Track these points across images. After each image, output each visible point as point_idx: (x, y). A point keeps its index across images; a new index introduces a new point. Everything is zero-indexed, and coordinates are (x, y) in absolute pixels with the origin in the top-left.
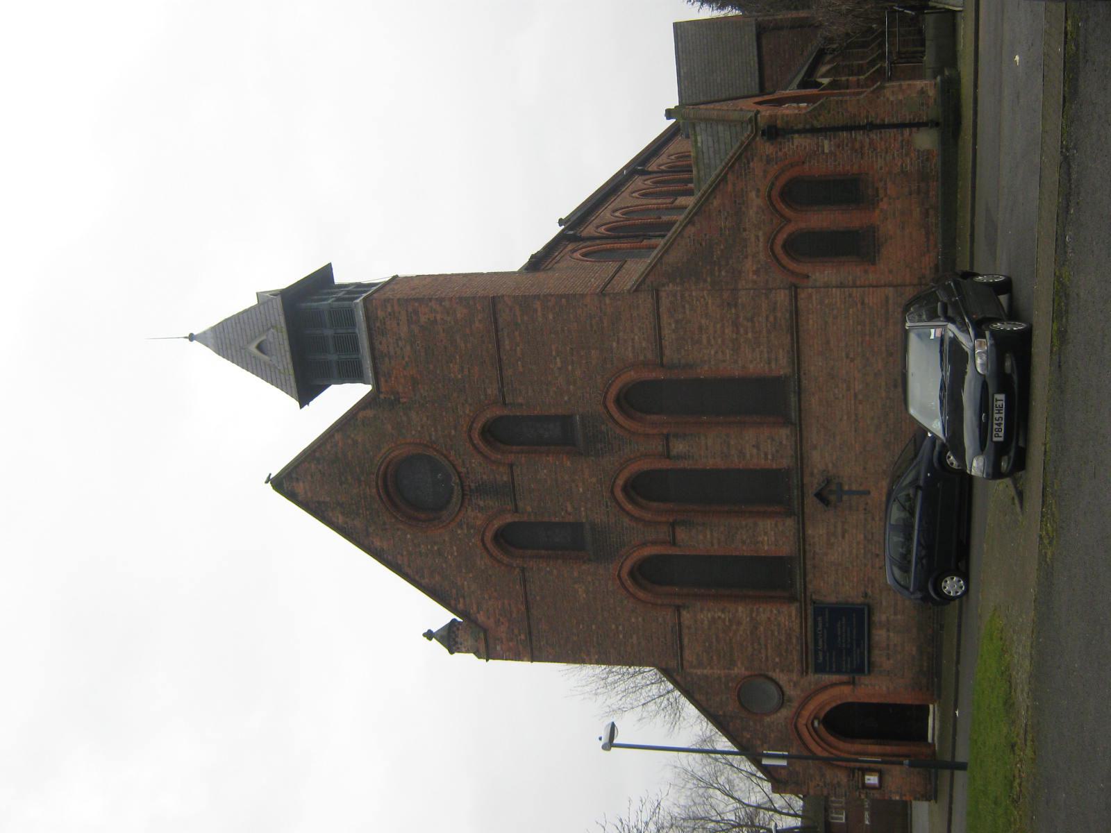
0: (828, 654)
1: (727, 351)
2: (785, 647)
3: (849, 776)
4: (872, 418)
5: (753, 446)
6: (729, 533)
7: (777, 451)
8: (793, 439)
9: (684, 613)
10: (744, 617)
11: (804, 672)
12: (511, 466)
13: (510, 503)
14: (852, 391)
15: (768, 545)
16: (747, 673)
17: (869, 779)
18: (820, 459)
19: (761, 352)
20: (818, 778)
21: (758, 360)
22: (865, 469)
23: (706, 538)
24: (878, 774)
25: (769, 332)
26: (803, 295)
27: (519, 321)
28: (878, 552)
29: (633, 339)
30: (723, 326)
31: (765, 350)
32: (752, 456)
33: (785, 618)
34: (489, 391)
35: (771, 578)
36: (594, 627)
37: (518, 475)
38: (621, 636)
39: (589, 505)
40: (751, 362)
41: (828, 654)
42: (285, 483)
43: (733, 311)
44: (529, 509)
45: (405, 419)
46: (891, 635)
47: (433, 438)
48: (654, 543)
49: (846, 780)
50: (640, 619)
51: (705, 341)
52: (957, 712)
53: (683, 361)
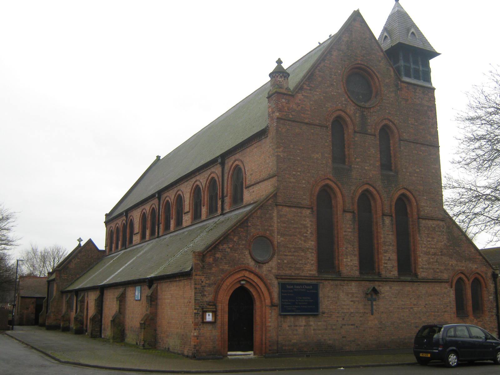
0: (292, 291)
1: (425, 249)
2: (293, 266)
3: (210, 302)
4: (403, 316)
5: (389, 258)
6: (351, 241)
7: (388, 269)
8: (393, 278)
9: (309, 211)
10: (308, 245)
11: (277, 277)
12: (375, 135)
13: (358, 130)
14: (413, 306)
15: (346, 261)
16: (275, 243)
17: (209, 315)
18: (385, 289)
19: (425, 265)
20: (208, 282)
21: (423, 263)
22: (383, 312)
23: (346, 229)
24: (213, 321)
25: (433, 269)
26: (446, 285)
27: (431, 156)
28: (345, 319)
29: (428, 207)
30: (434, 248)
31: (426, 267)
32: (385, 256)
33: (309, 268)
34: (404, 134)
35: (327, 261)
36: (299, 158)
37: (371, 138)
38: (294, 173)
39: (360, 171)
40: (422, 260)
41: (292, 291)
42: (356, 17)
43: (440, 254)
44: (356, 139)
45: (391, 90)
46: (303, 328)
47: (384, 101)
48: (344, 201)
49: (207, 300)
50: (304, 186)
51: (429, 239)
52: (342, 368)
53: (421, 228)
